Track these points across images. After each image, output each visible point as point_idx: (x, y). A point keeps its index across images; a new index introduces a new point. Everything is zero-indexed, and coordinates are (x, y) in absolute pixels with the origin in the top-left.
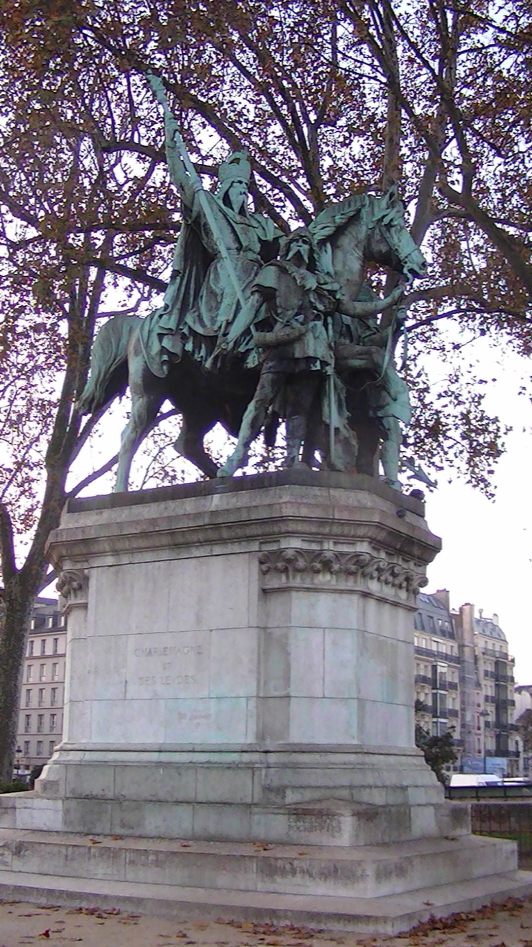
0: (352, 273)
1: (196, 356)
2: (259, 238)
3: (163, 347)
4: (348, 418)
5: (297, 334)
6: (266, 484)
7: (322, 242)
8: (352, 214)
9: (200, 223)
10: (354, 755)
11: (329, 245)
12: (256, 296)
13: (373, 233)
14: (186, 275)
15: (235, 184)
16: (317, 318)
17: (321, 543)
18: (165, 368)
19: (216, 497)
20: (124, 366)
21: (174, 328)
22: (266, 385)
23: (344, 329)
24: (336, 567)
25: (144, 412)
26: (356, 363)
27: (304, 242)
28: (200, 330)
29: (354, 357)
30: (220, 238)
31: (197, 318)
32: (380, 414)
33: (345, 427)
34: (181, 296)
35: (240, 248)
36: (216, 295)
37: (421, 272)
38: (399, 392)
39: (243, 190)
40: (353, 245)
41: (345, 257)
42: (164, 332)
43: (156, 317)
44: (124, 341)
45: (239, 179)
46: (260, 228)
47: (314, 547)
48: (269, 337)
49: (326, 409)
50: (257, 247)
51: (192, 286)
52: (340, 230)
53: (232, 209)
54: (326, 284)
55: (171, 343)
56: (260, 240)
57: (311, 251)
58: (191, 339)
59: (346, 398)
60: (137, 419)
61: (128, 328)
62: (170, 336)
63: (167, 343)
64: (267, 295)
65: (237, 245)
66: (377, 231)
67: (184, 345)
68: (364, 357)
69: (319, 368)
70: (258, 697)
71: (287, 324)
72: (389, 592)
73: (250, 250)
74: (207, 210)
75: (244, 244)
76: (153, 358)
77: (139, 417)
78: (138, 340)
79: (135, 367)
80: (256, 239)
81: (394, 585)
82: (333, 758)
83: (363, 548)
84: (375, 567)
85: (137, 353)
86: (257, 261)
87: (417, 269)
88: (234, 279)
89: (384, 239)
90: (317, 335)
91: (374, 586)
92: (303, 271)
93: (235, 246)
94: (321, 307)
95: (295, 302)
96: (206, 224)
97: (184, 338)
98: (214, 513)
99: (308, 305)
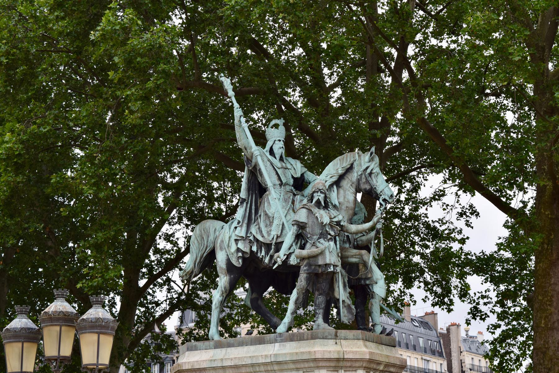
0: (348, 202)
1: (259, 254)
2: (292, 176)
3: (238, 248)
4: (350, 293)
5: (320, 251)
6: (305, 337)
7: (331, 186)
8: (349, 166)
9: (256, 169)
11: (335, 187)
12: (295, 227)
13: (361, 178)
14: (249, 201)
15: (276, 142)
17: (337, 371)
18: (240, 261)
19: (277, 345)
20: (212, 255)
21: (244, 236)
22: (303, 280)
23: (345, 238)
25: (228, 286)
26: (354, 260)
27: (321, 192)
28: (261, 239)
29: (352, 256)
30: (268, 178)
31: (258, 230)
32: (368, 282)
33: (348, 298)
34: (247, 214)
35: (281, 184)
36: (269, 217)
37: (390, 201)
38: (377, 279)
40: (349, 185)
41: (345, 193)
42: (239, 238)
43: (233, 227)
44: (211, 238)
45: (279, 139)
46: (293, 169)
48: (305, 252)
49: (337, 289)
50: (291, 181)
51: (253, 207)
52: (341, 177)
53: (276, 158)
54: (335, 217)
55: (243, 246)
56: (293, 177)
57: (326, 197)
58: (255, 244)
59: (348, 281)
60: (223, 289)
61: (214, 230)
62: (242, 241)
63: (241, 245)
64: (301, 226)
65: (280, 182)
66: (363, 176)
67: (251, 247)
68: (358, 257)
69: (332, 270)
71: (314, 245)
73: (287, 184)
74: (259, 160)
75: (284, 182)
76: (232, 254)
77: (225, 288)
78: (222, 241)
80: (290, 177)
85: (221, 249)
86: (291, 191)
87: (387, 198)
88: (280, 207)
89: (367, 182)
90: (331, 250)
92: (322, 212)
93: (278, 182)
94: (332, 233)
95: (318, 231)
96: (260, 170)
97: (251, 242)
98: (276, 355)
99: (325, 232)
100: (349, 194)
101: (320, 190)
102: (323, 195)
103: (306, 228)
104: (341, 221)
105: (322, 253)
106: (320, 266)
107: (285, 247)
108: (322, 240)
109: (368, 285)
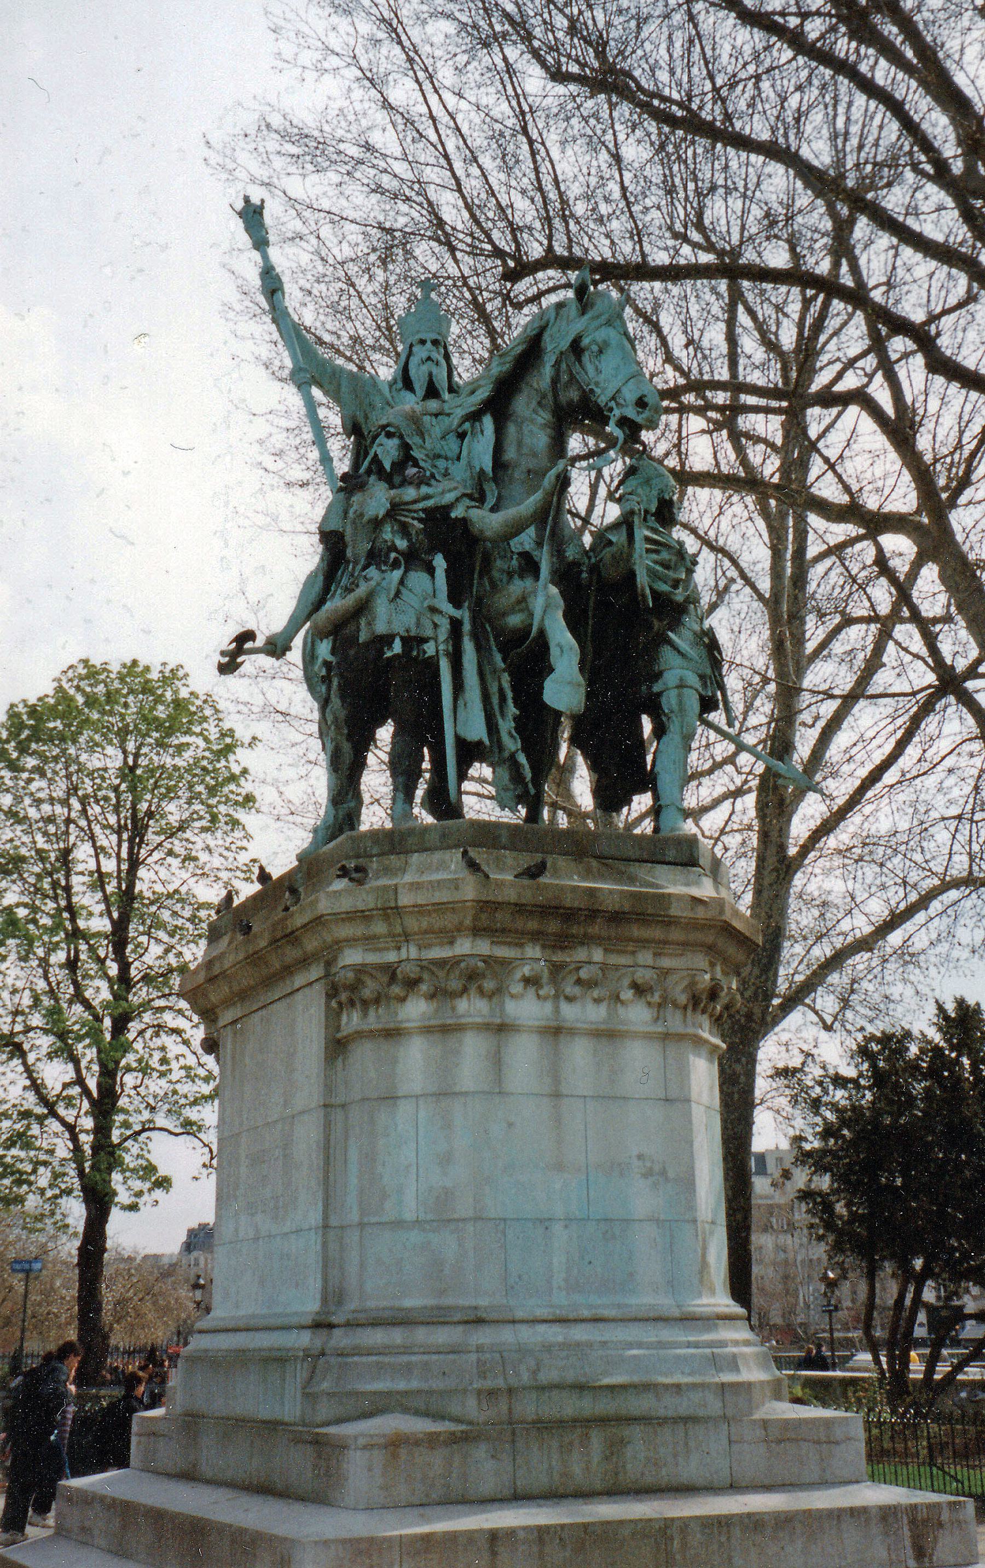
0: (535, 455)
7: (474, 417)
10: (556, 1328)
11: (488, 422)
16: (395, 565)
17: (399, 948)
23: (514, 562)
24: (424, 987)
27: (389, 435)
32: (656, 688)
39: (424, 355)
40: (534, 403)
45: (418, 337)
47: (392, 957)
57: (406, 447)
70: (326, 1226)
72: (586, 1012)
81: (597, 1001)
82: (421, 1335)
83: (464, 946)
84: (518, 975)
87: (631, 412)
89: (572, 378)
91: (527, 1009)
94: (402, 544)
100: (535, 430)
101: (383, 427)
102: (393, 443)
103: (345, 546)
104: (450, 506)
105: (363, 608)
106: (367, 644)
108: (372, 572)
109: (659, 694)
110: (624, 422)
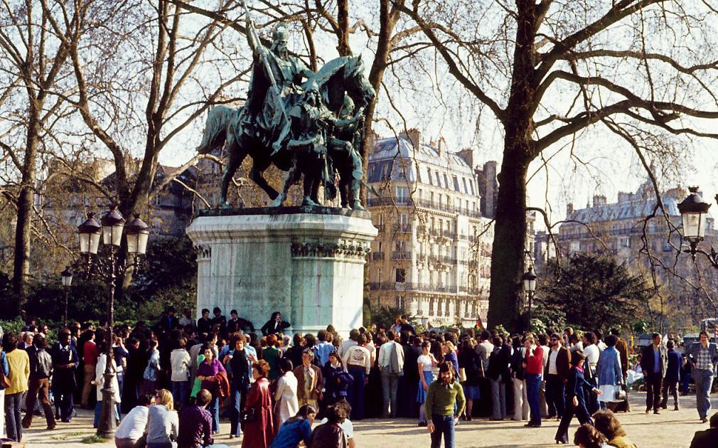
36: (271, 108)
44: (223, 122)
63: (246, 131)
78: (232, 126)
79: (230, 137)
107: (282, 136)
110: (367, 99)
